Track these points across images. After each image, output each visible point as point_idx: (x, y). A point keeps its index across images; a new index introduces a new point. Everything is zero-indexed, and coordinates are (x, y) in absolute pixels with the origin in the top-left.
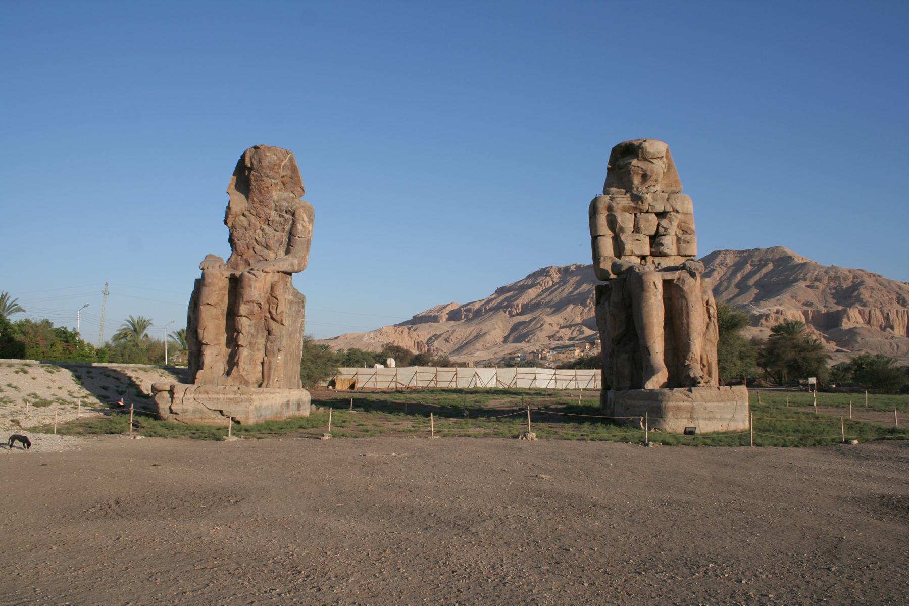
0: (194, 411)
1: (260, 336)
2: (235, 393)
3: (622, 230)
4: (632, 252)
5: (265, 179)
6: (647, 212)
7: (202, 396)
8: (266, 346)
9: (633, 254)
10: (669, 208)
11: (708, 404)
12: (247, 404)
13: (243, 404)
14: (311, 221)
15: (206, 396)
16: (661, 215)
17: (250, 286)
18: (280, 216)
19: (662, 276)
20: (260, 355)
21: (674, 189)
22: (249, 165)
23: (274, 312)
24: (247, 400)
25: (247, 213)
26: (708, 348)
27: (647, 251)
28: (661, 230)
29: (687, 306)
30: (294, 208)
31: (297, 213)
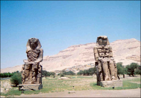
10: (108, 48)
14: (43, 52)
16: (106, 49)
31: (41, 51)
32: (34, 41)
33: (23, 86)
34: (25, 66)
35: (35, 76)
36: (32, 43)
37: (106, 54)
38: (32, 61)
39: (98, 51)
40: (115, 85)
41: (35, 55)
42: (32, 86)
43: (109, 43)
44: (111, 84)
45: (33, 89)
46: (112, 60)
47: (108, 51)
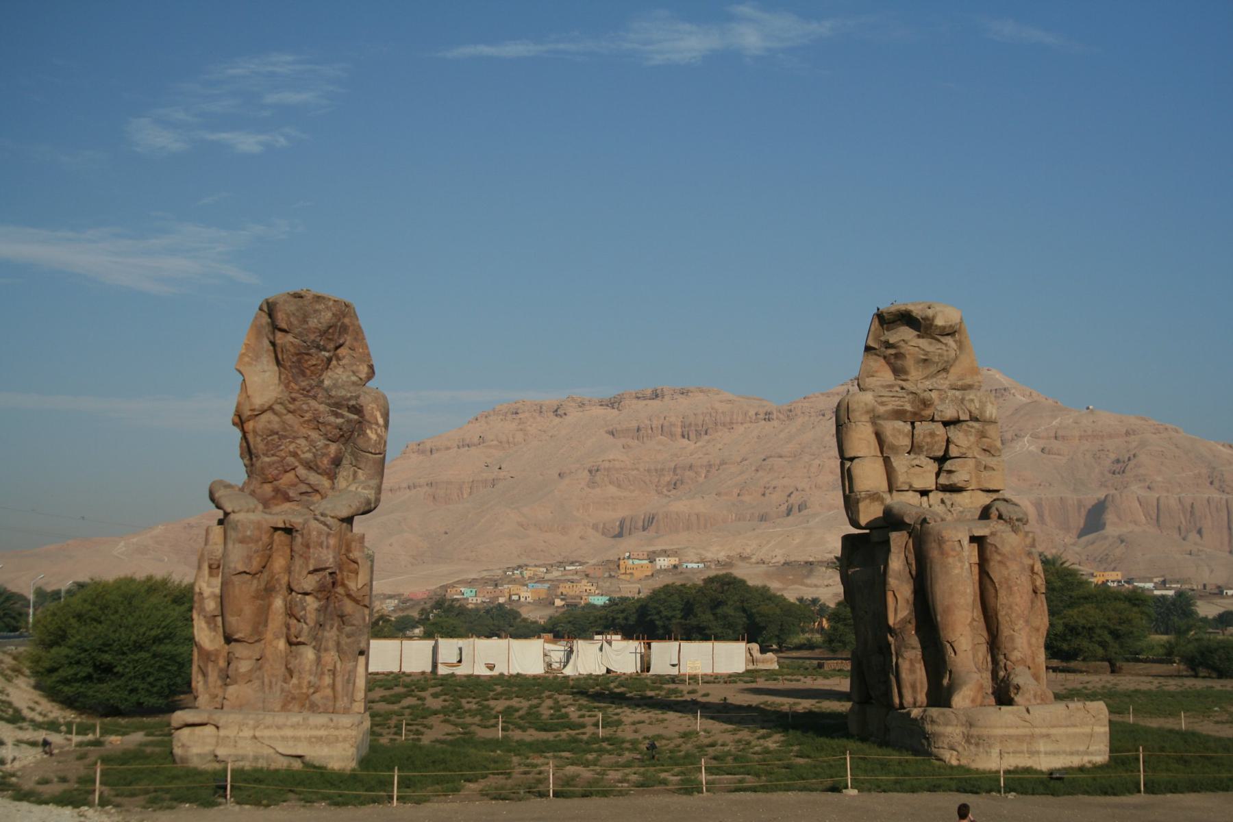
0: (256, 758)
1: (328, 628)
2: (325, 727)
3: (894, 449)
4: (911, 486)
5: (313, 351)
6: (933, 420)
7: (267, 733)
8: (338, 644)
9: (911, 488)
11: (1053, 731)
12: (347, 745)
13: (340, 745)
15: (277, 733)
17: (321, 545)
18: (337, 415)
19: (970, 530)
20: (330, 657)
21: (968, 381)
22: (284, 326)
23: (352, 585)
24: (345, 740)
25: (277, 407)
26: (1034, 640)
27: (929, 482)
28: (953, 451)
29: (1007, 580)
30: (362, 401)
32: (313, 322)
33: (218, 728)
34: (230, 546)
35: (315, 638)
36: (290, 338)
37: (948, 465)
38: (288, 499)
39: (879, 436)
40: (1042, 746)
41: (312, 443)
42: (301, 733)
43: (975, 371)
44: (1010, 737)
45: (307, 759)
46: (1009, 521)
47: (962, 439)
